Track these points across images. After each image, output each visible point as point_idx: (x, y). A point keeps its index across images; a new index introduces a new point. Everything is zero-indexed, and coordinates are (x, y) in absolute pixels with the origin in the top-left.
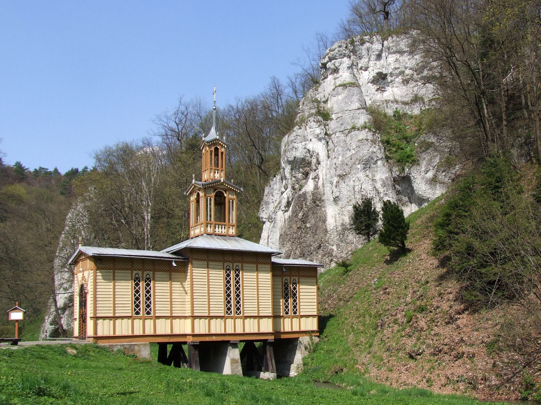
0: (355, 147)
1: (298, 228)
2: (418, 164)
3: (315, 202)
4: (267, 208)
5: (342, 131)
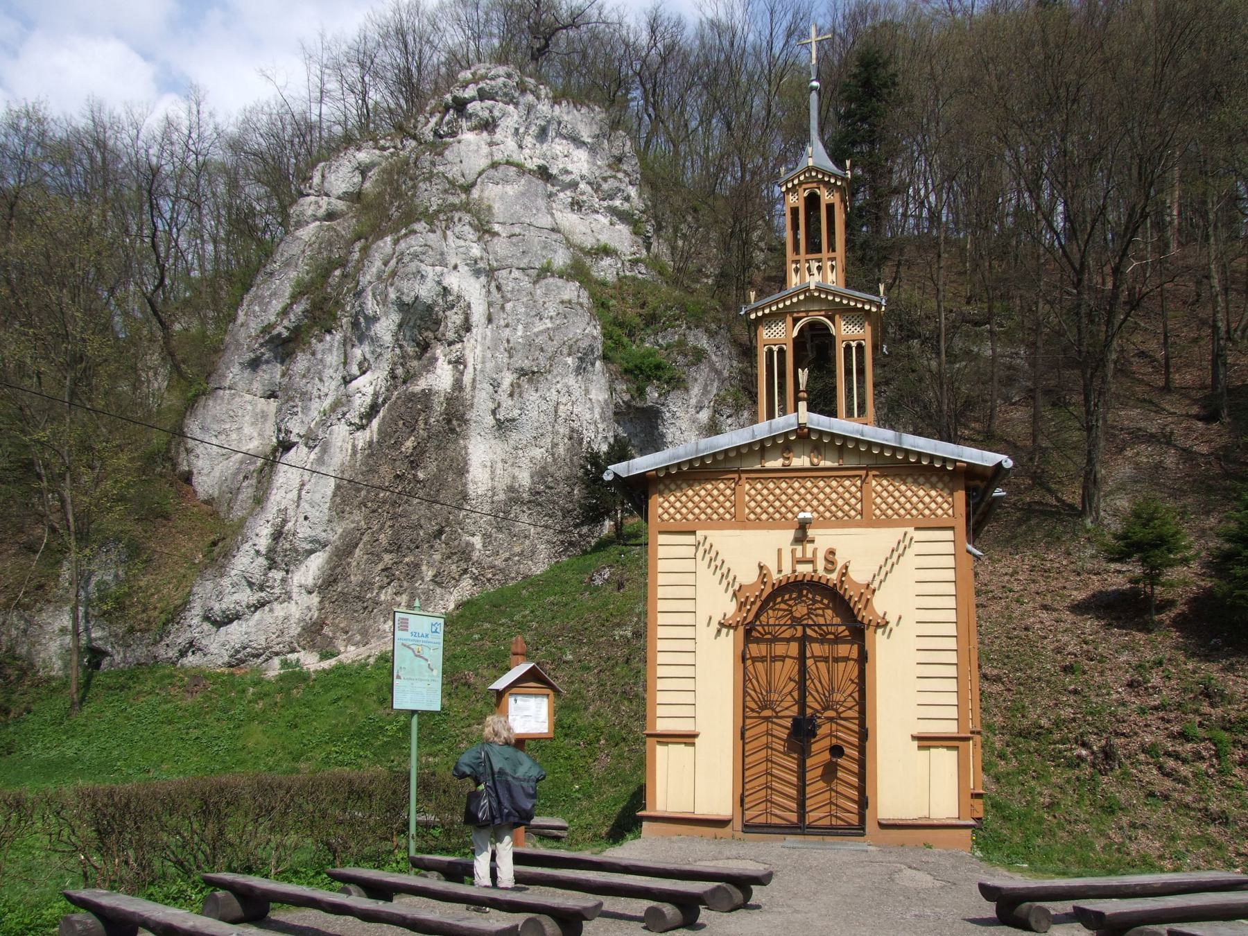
2: (687, 390)
3: (449, 422)
5: (523, 269)
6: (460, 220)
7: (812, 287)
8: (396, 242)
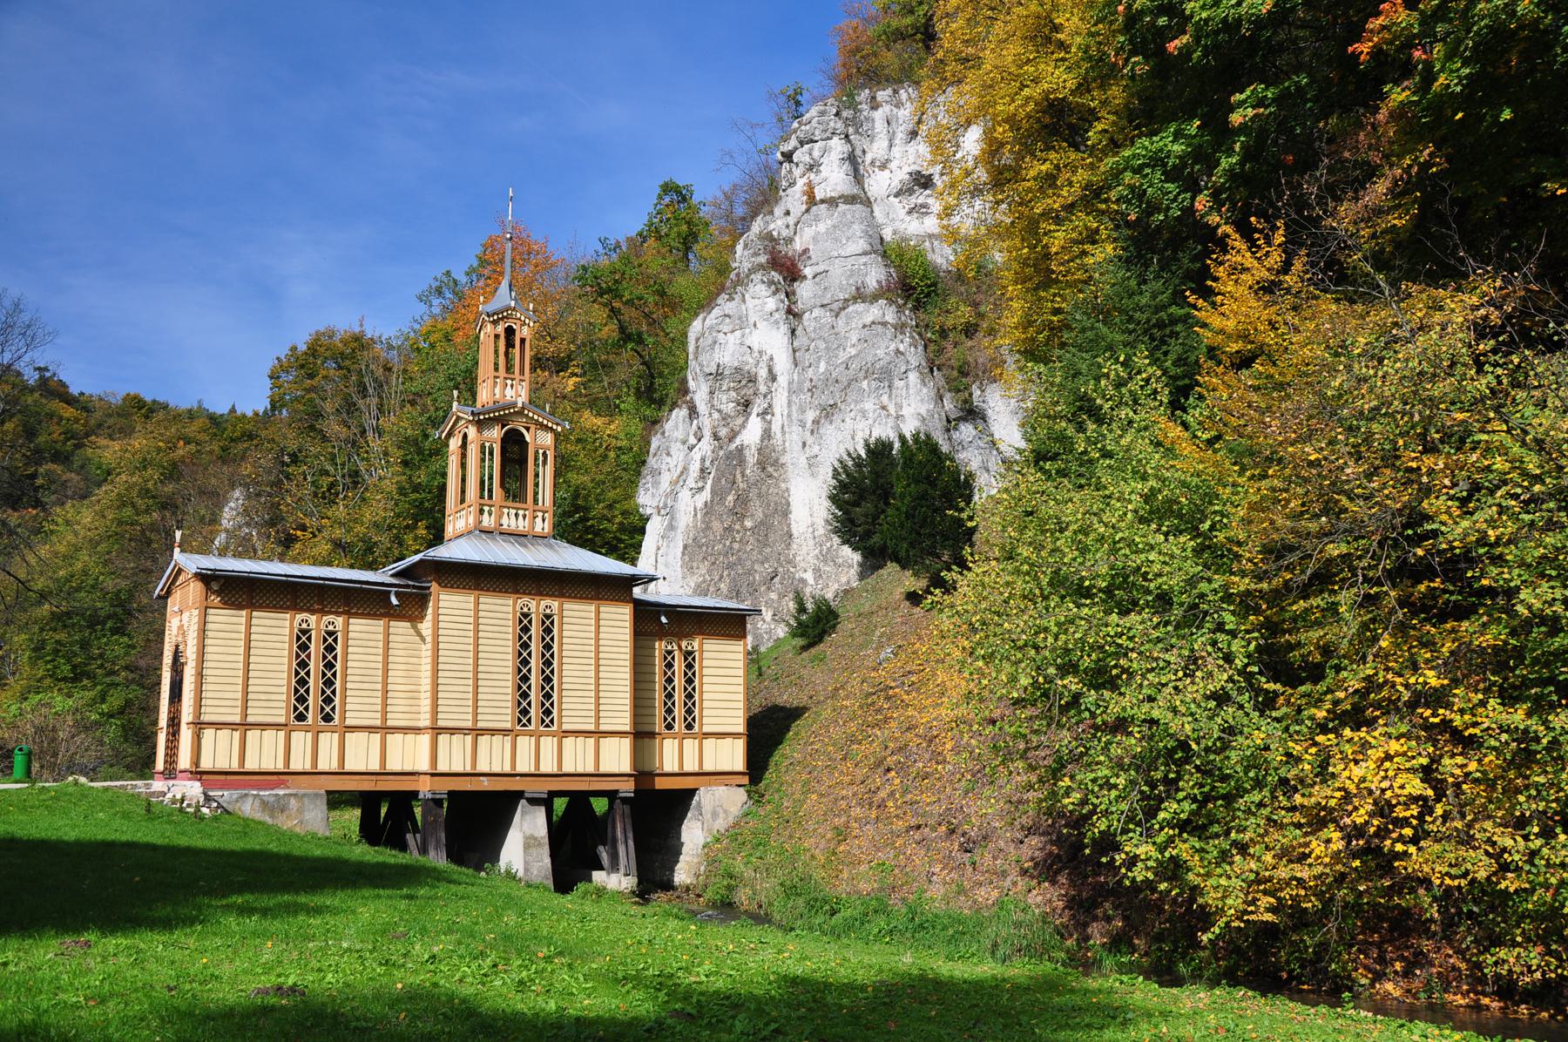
0: (854, 340)
1: (725, 529)
3: (764, 469)
4: (656, 484)
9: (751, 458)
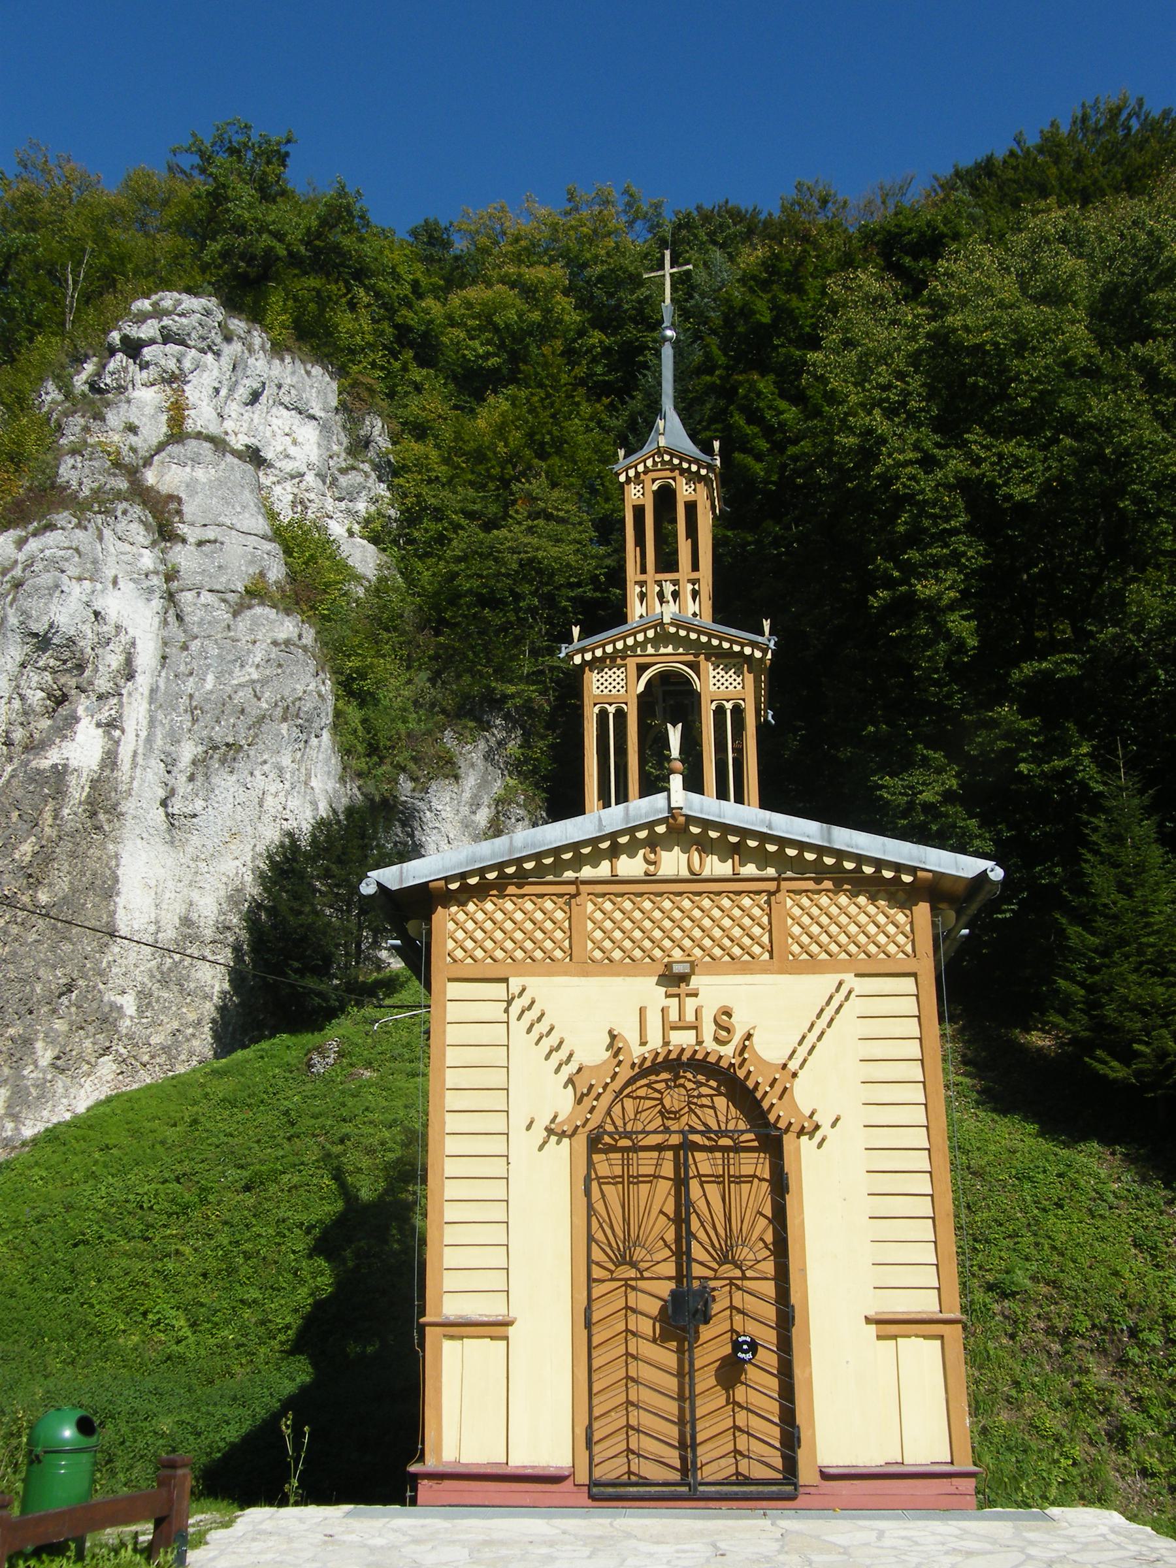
3: (93, 815)
6: (125, 513)
7: (666, 620)
8: (21, 543)
9: (77, 791)
